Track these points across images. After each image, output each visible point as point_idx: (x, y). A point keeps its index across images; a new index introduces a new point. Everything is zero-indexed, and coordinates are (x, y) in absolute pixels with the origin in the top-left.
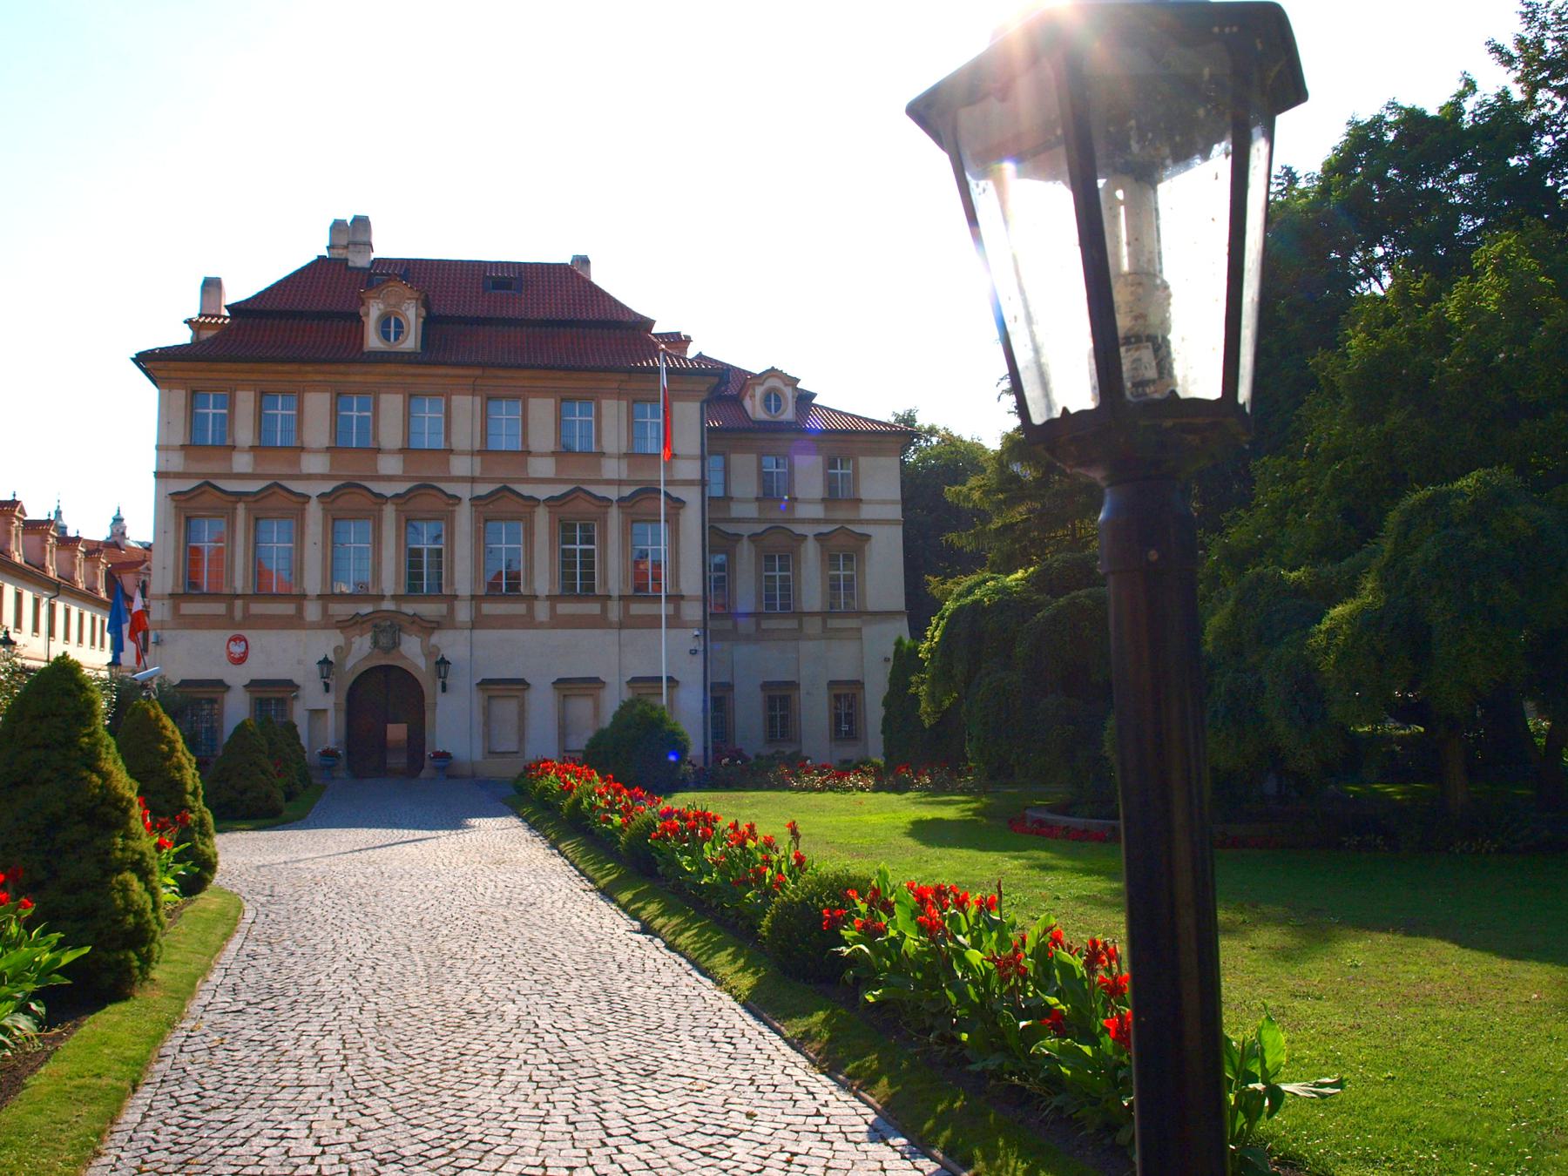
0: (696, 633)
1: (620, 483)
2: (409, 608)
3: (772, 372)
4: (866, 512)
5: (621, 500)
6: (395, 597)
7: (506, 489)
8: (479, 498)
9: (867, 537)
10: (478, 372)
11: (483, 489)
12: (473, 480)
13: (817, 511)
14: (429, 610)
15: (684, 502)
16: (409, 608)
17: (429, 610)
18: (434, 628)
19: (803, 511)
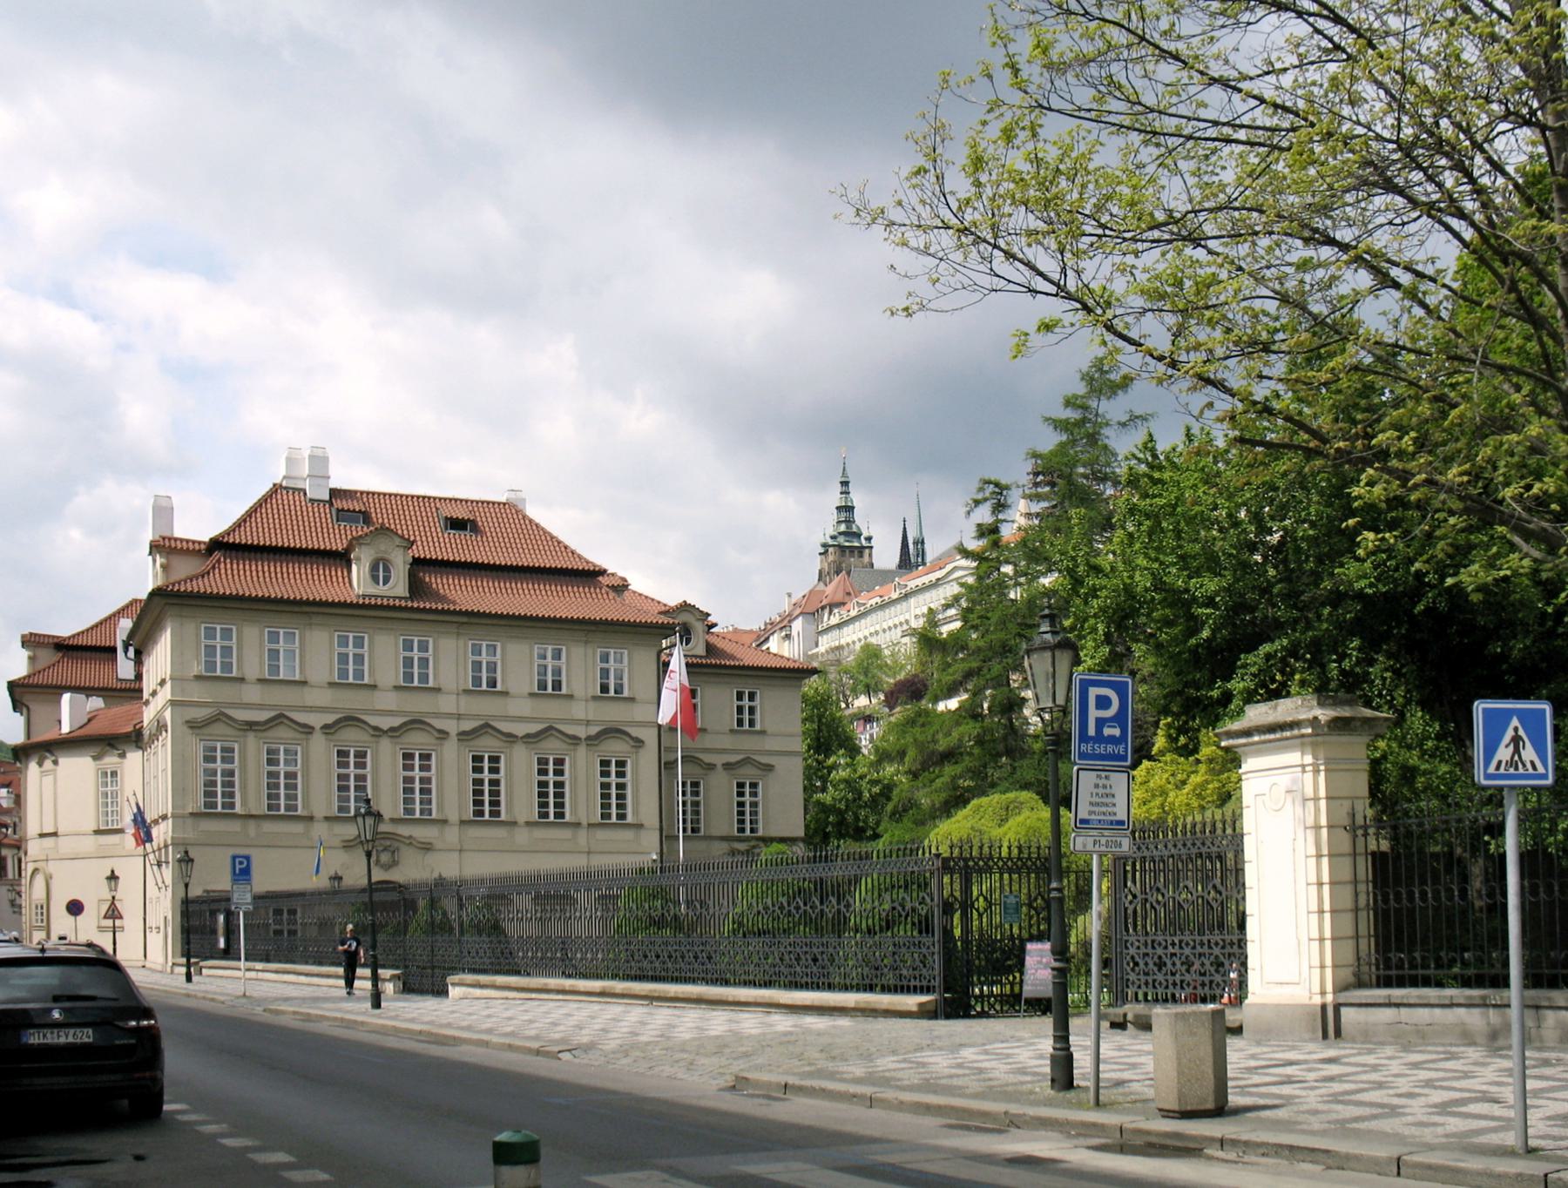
0: (655, 857)
1: (588, 723)
2: (404, 830)
3: (685, 607)
4: (771, 744)
5: (589, 738)
6: (393, 820)
7: (487, 725)
8: (463, 733)
9: (769, 768)
10: (465, 619)
11: (468, 725)
12: (459, 717)
13: (727, 742)
14: (421, 833)
15: (642, 742)
16: (404, 830)
17: (421, 833)
18: (428, 849)
19: (707, 741)
